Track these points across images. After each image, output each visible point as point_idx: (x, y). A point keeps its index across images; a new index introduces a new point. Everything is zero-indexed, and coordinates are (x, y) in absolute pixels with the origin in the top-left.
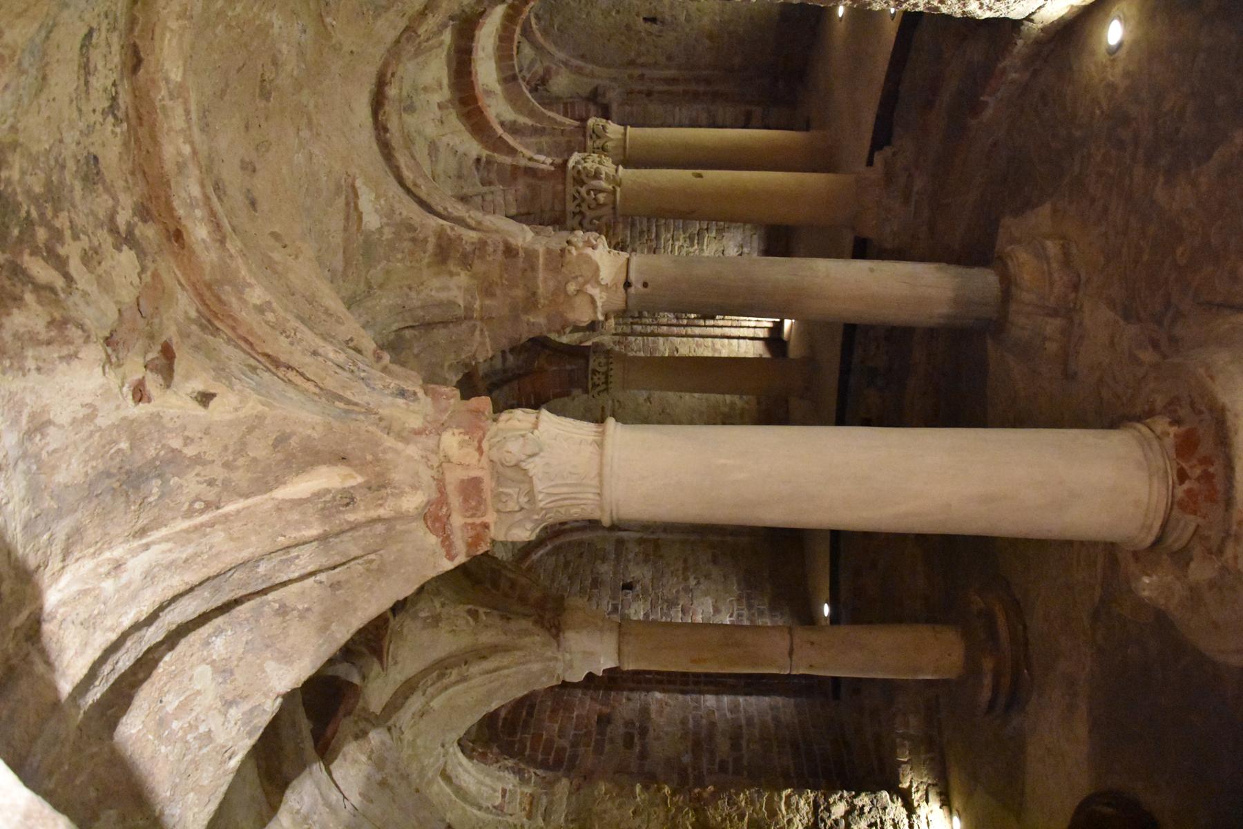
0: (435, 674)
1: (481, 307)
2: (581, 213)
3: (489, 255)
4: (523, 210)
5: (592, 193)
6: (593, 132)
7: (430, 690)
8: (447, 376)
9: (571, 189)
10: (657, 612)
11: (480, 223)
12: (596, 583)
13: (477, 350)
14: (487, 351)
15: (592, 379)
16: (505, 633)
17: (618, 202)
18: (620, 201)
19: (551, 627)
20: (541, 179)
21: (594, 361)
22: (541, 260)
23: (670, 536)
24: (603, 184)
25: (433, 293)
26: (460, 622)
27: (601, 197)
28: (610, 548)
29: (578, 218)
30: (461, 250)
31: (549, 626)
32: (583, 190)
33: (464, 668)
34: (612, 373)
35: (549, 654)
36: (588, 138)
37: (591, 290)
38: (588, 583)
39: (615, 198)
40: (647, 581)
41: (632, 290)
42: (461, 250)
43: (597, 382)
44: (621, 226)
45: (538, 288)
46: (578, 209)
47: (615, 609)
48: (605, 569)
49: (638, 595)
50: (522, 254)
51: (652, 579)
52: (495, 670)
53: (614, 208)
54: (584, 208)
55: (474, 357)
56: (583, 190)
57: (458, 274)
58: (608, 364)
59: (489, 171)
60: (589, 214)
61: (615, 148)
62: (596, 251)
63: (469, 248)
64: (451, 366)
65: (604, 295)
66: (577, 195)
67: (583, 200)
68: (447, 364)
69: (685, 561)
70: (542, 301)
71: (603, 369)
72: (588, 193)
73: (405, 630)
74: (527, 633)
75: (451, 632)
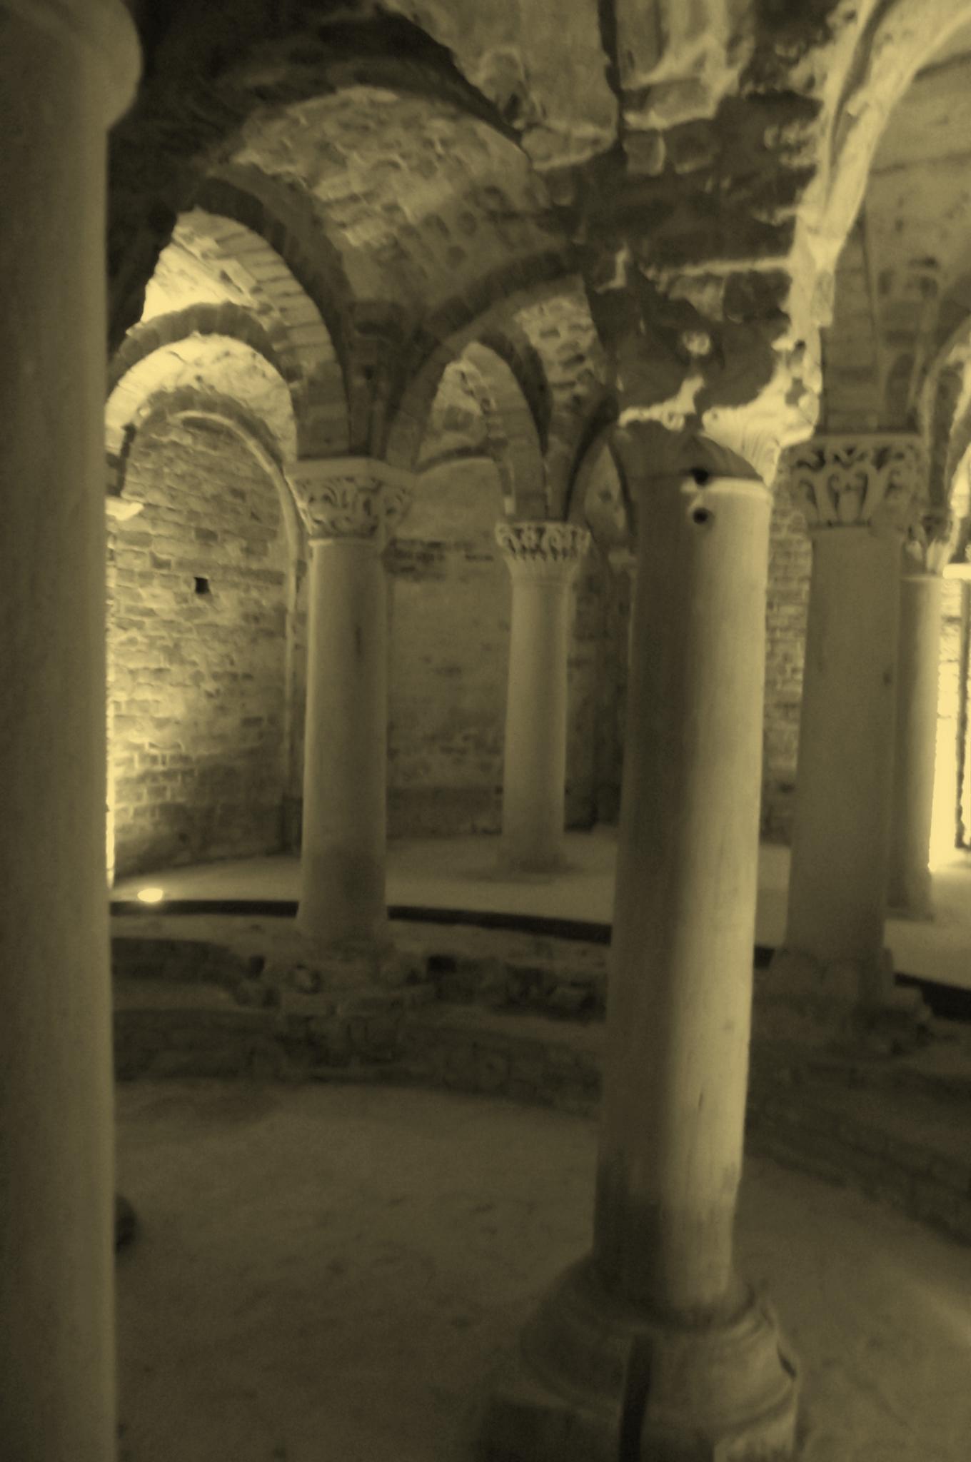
1: (653, 133)
3: (778, 137)
8: (487, 57)
10: (156, 629)
11: (852, 121)
12: (207, 537)
13: (549, 130)
14: (548, 157)
15: (529, 528)
22: (765, 265)
23: (289, 655)
28: (268, 563)
30: (793, 52)
34: (538, 557)
37: (691, 387)
38: (207, 525)
40: (211, 617)
41: (690, 486)
42: (793, 52)
43: (524, 537)
45: (696, 262)
47: (159, 564)
48: (232, 552)
49: (186, 601)
50: (782, 214)
51: (217, 626)
54: (830, 469)
55: (531, 126)
57: (731, 62)
58: (554, 550)
62: (781, 400)
63: (797, 76)
64: (510, 62)
65: (677, 424)
68: (514, 51)
69: (248, 677)
70: (665, 277)
71: (545, 545)
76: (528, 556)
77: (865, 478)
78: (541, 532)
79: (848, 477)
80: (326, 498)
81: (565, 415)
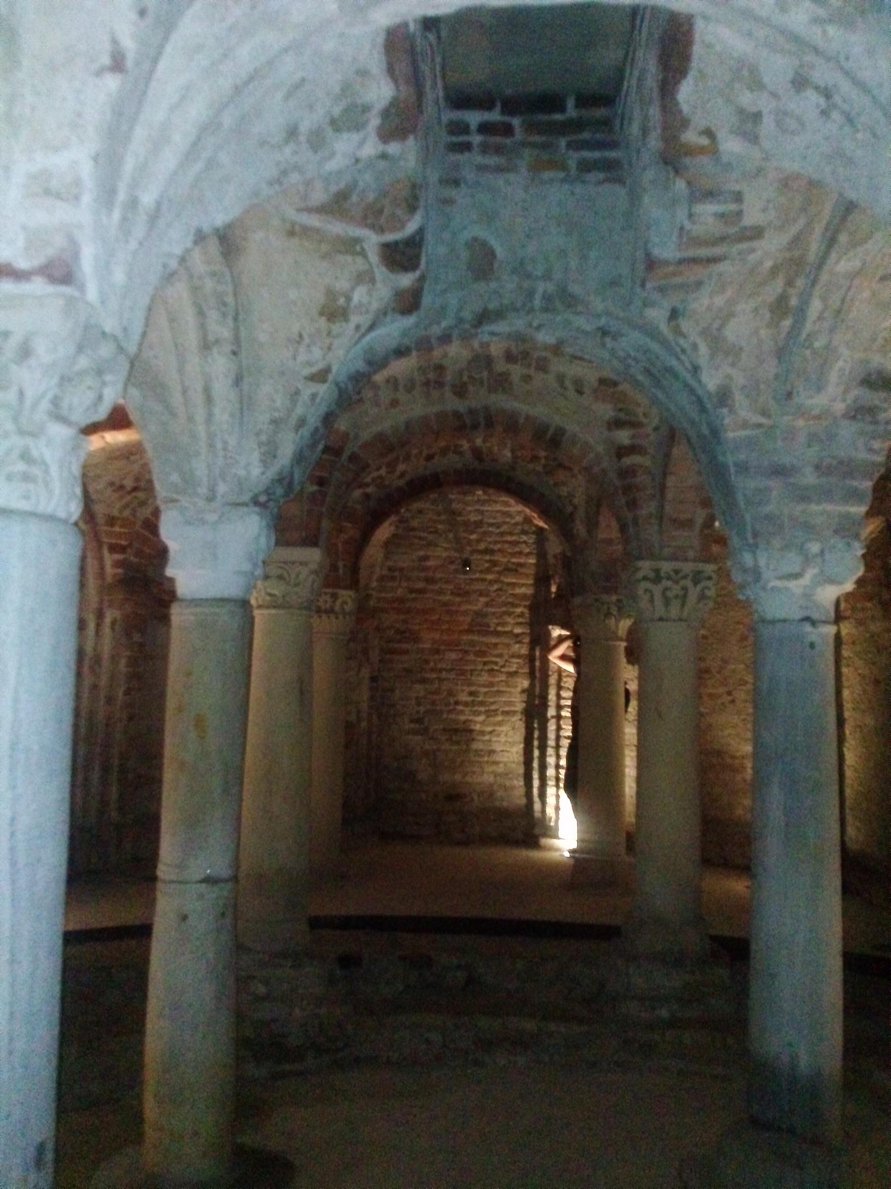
0: (230, 299)
7: (209, 285)
9: (688, 567)
15: (326, 594)
16: (274, 422)
19: (269, 494)
21: (350, 596)
25: (840, 363)
26: (317, 353)
29: (652, 575)
31: (270, 492)
32: (688, 583)
33: (228, 348)
34: (333, 617)
35: (222, 488)
37: (810, 573)
44: (437, 636)
52: (209, 400)
53: (661, 619)
54: (666, 583)
58: (344, 613)
64: (729, 377)
66: (681, 575)
71: (337, 608)
73: (349, 258)
74: (270, 453)
75: (301, 336)
76: (324, 617)
77: (685, 589)
78: (335, 596)
79: (676, 590)
80: (280, 577)
81: (359, 507)
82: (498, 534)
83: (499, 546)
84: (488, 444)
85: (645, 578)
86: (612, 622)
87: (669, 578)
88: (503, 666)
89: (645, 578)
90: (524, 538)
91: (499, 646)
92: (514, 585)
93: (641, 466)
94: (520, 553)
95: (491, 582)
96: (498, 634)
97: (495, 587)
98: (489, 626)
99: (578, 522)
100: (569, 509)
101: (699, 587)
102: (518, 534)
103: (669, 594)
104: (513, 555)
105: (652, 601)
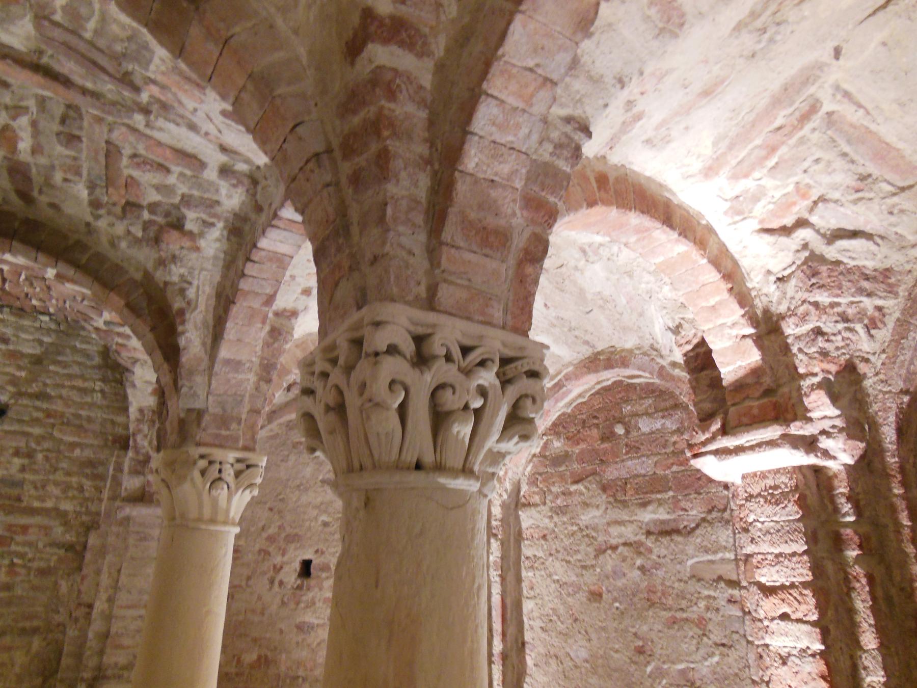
2: (422, 360)
4: (462, 188)
5: (477, 403)
6: (248, 467)
17: (443, 480)
18: (444, 489)
20: (520, 264)
24: (491, 442)
27: (463, 429)
29: (409, 347)
32: (488, 377)
36: (239, 455)
39: (455, 473)
46: (437, 347)
53: (418, 466)
54: (441, 371)
56: (488, 377)
59: (559, 146)
60: (429, 378)
61: (215, 503)
66: (474, 357)
67: (467, 372)
72: (483, 392)
82: (64, 375)
83: (64, 392)
84: (43, 160)
85: (392, 350)
86: (222, 493)
87: (448, 358)
88: (30, 560)
89: (392, 350)
90: (99, 385)
91: (31, 530)
92: (73, 446)
93: (409, 79)
94: (91, 406)
95: (40, 439)
96: (32, 511)
97: (46, 445)
98: (19, 499)
99: (189, 326)
100: (177, 304)
101: (513, 392)
102: (94, 381)
103: (450, 401)
104: (82, 406)
105: (402, 410)
